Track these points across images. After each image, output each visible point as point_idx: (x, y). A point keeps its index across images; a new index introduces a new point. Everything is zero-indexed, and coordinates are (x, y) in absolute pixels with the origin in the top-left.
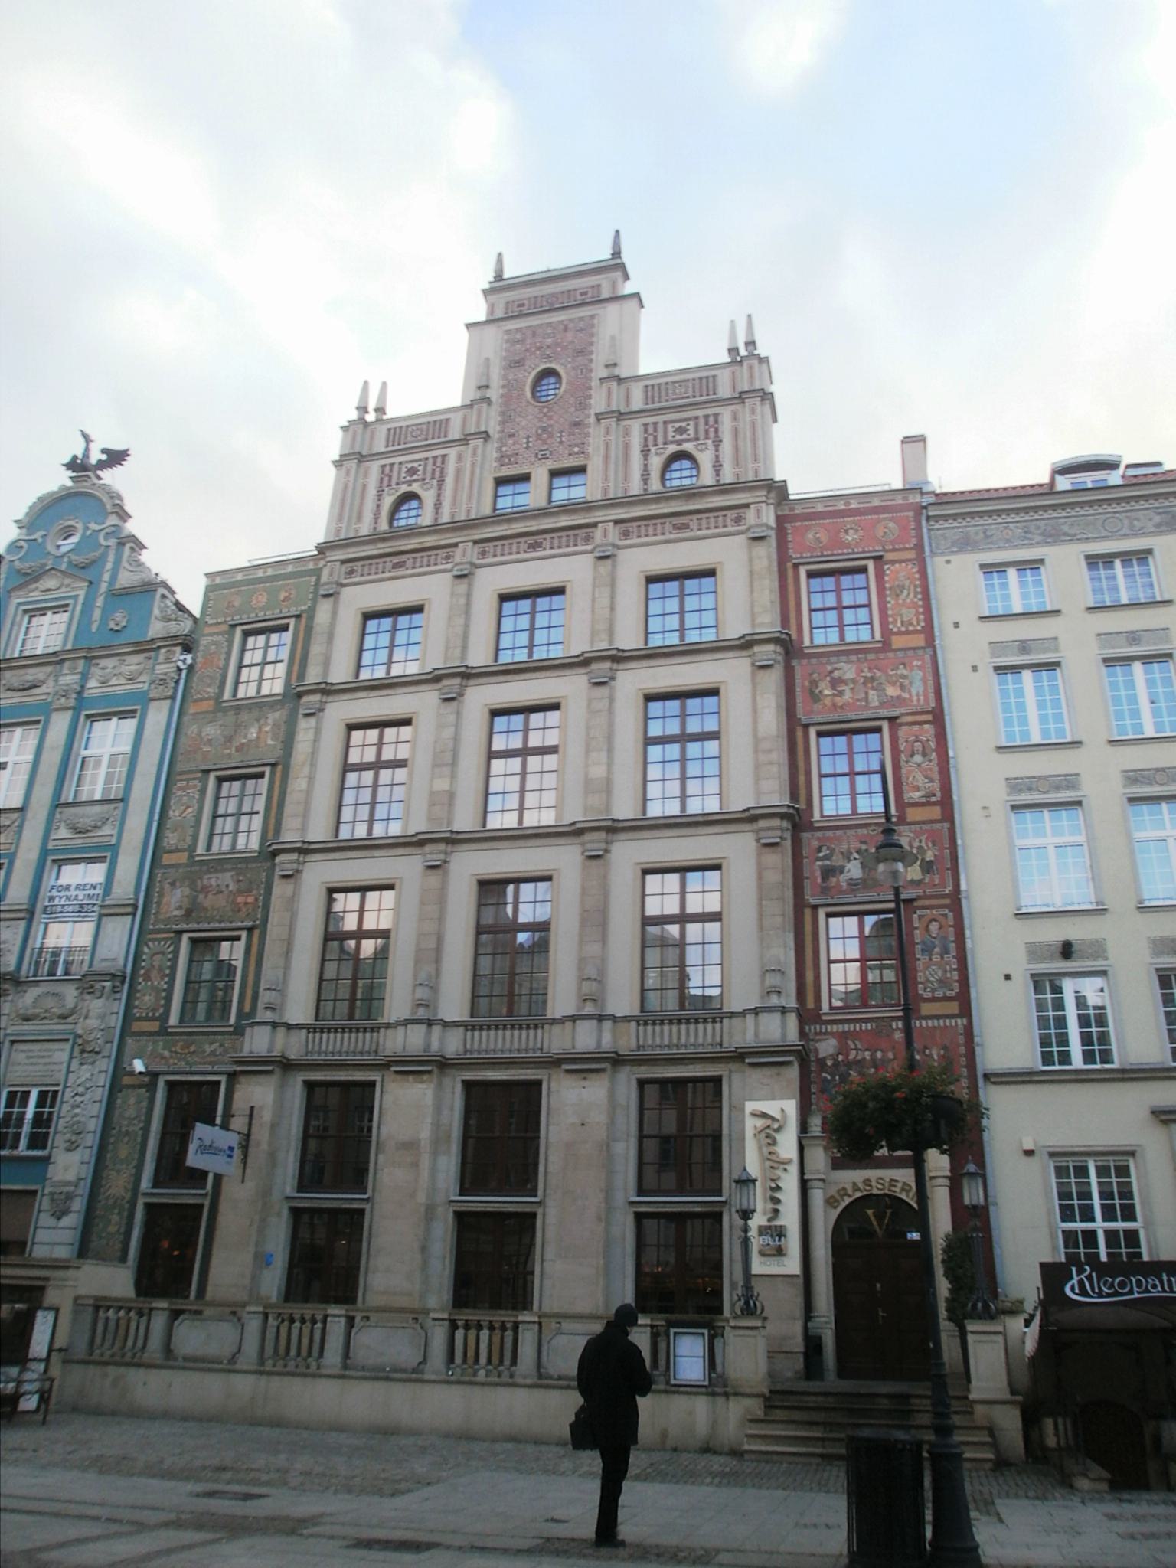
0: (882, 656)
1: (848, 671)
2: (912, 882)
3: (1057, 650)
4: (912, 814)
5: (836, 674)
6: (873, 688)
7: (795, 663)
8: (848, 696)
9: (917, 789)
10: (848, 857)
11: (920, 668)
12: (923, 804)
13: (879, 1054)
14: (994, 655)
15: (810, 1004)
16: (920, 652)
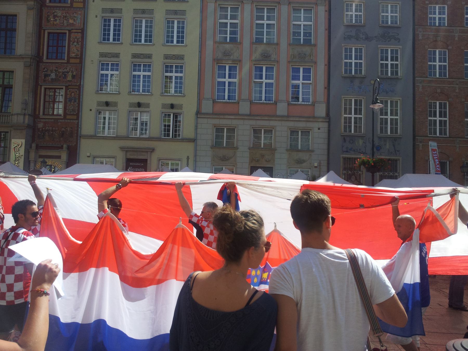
0: (69, 9)
1: (59, 13)
2: (69, 81)
3: (121, 13)
4: (72, 61)
5: (55, 14)
6: (66, 20)
7: (43, 8)
8: (58, 22)
9: (74, 53)
10: (52, 71)
11: (80, 14)
12: (74, 58)
13: (54, 128)
14: (103, 13)
15: (37, 113)
16: (81, 9)
